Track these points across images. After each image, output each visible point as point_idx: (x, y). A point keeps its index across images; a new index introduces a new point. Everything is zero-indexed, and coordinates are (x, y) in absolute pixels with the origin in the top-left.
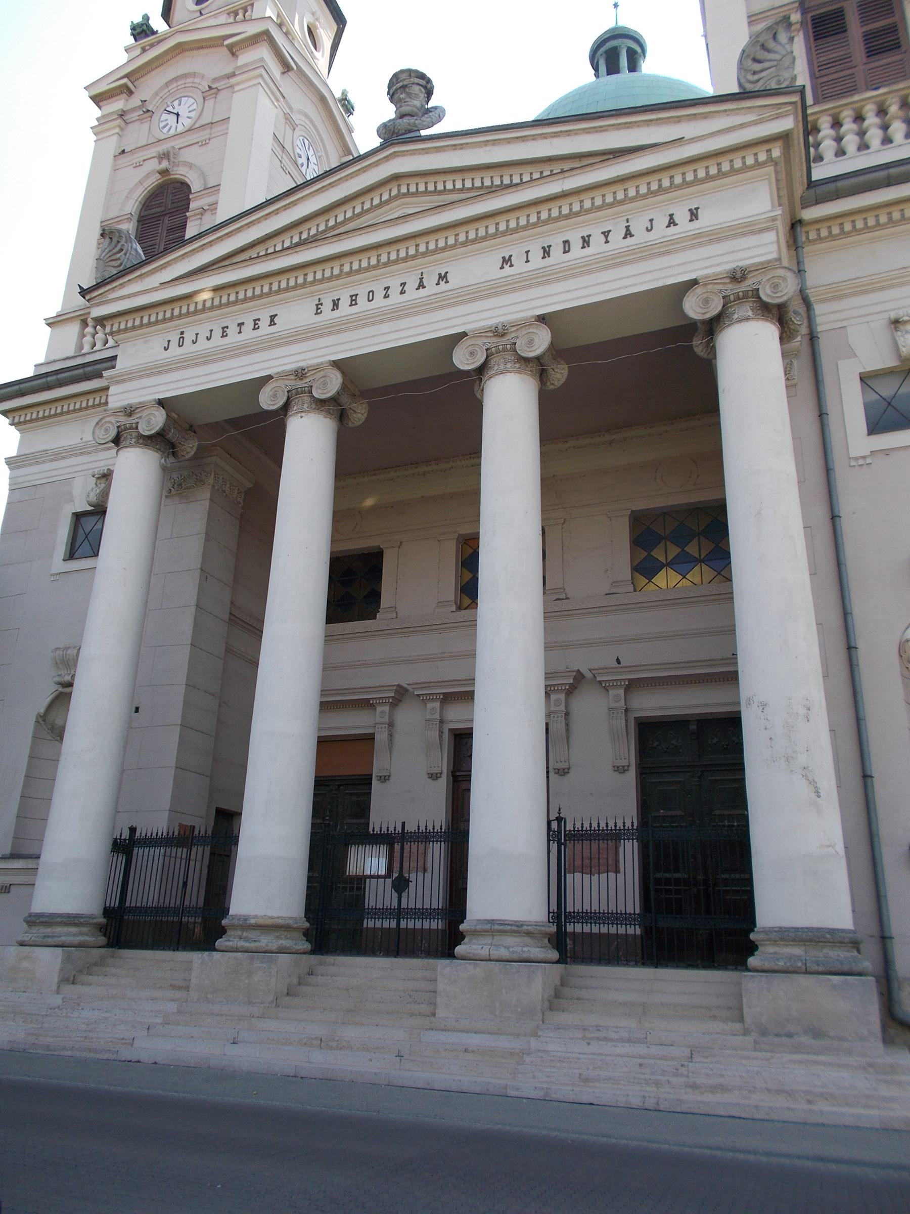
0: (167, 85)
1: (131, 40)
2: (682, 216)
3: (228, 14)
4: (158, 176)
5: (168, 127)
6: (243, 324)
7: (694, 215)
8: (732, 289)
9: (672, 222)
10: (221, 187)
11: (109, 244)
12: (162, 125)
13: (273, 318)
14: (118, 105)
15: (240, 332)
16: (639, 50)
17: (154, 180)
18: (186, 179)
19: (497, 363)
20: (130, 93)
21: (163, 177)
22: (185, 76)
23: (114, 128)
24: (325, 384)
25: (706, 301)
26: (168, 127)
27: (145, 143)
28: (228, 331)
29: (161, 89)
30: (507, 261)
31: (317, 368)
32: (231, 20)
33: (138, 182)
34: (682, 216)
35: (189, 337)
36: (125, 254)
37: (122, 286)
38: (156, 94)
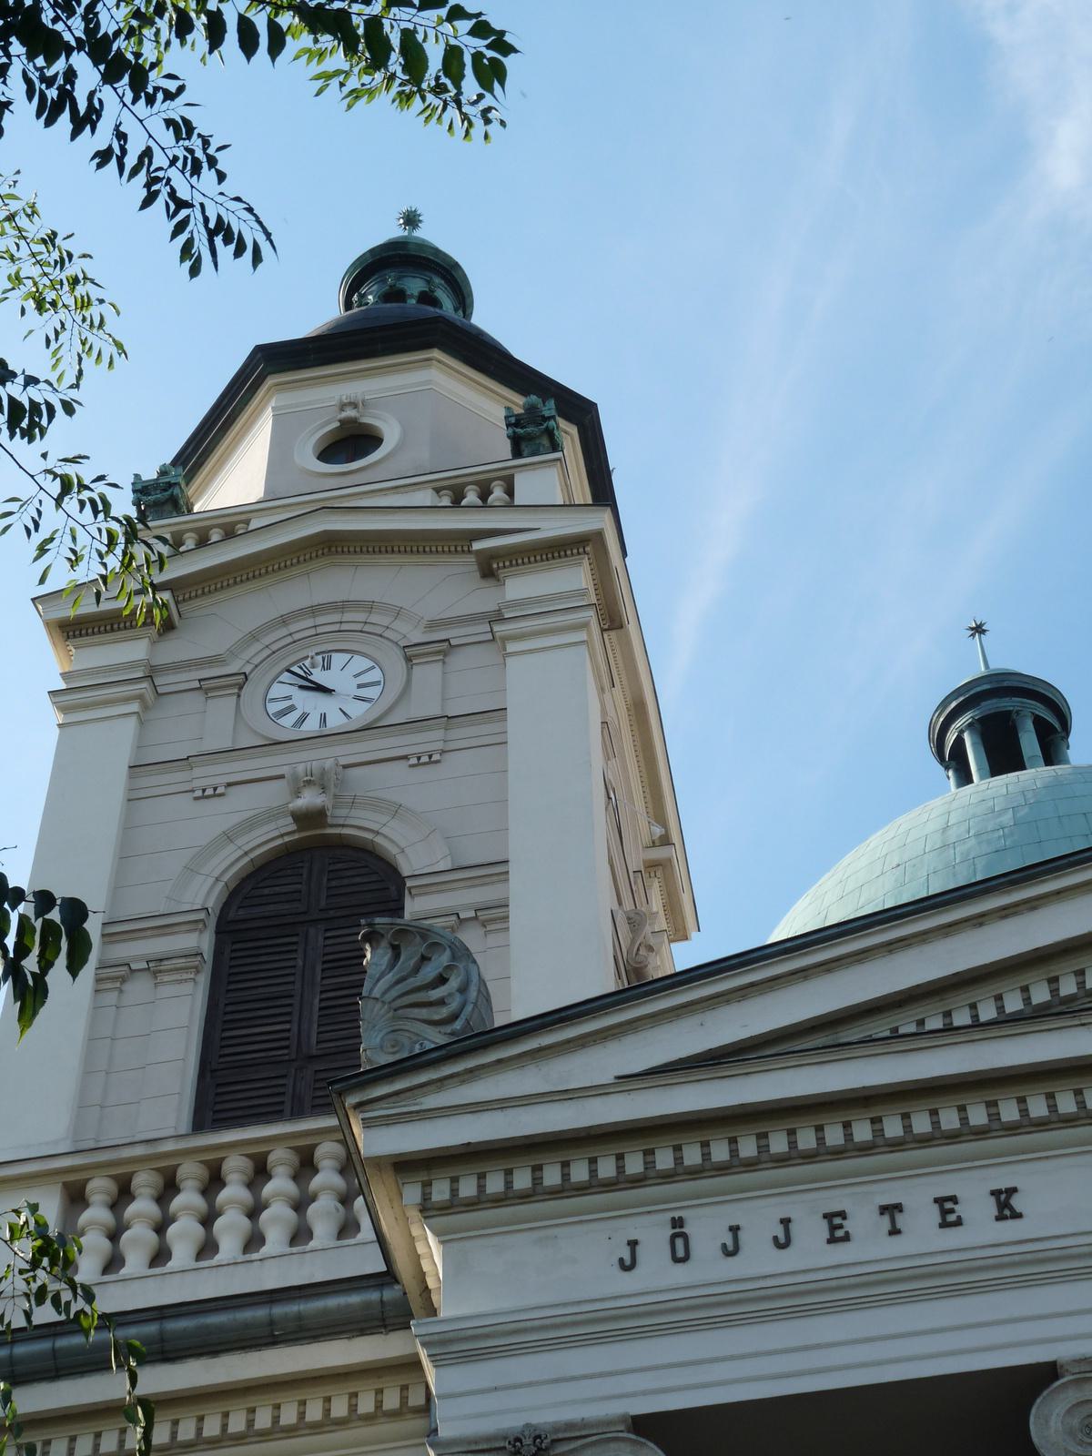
0: (284, 620)
3: (438, 490)
4: (288, 824)
5: (293, 717)
6: (898, 1208)
10: (512, 868)
11: (392, 965)
12: (273, 708)
15: (895, 1231)
18: (379, 840)
20: (168, 626)
21: (299, 830)
22: (342, 606)
23: (127, 700)
26: (293, 717)
27: (228, 745)
28: (849, 1225)
32: (446, 501)
35: (706, 1229)
36: (463, 990)
37: (472, 1074)
38: (253, 637)
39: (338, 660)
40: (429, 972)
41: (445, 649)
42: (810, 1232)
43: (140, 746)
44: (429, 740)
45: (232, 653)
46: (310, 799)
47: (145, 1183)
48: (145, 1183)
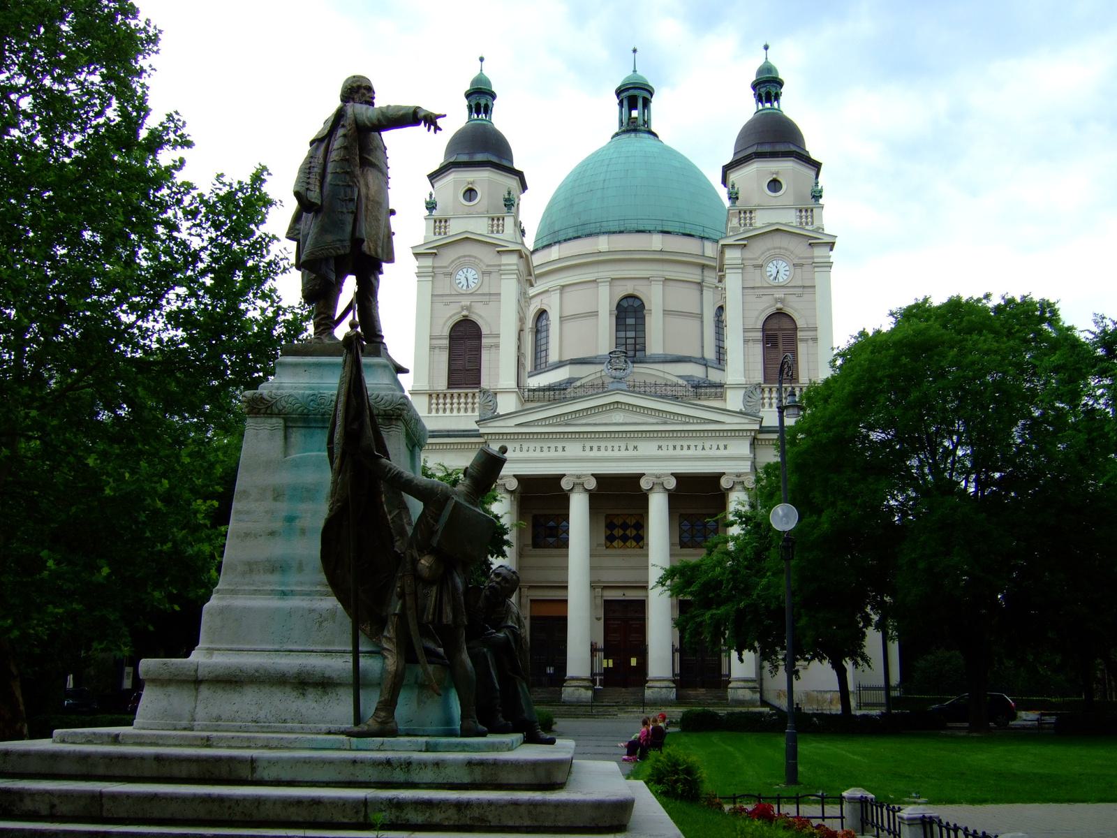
0: (459, 258)
1: (427, 213)
2: (722, 447)
7: (725, 447)
8: (737, 479)
9: (718, 448)
12: (458, 281)
13: (564, 448)
14: (428, 262)
16: (648, 96)
17: (457, 318)
19: (657, 488)
22: (469, 256)
23: (429, 276)
24: (589, 483)
25: (728, 482)
29: (455, 260)
30: (660, 447)
31: (585, 475)
33: (449, 316)
34: (722, 447)
35: (525, 447)
38: (453, 262)
39: (470, 270)
40: (489, 399)
41: (490, 273)
42: (538, 449)
43: (432, 291)
44: (486, 298)
45: (449, 265)
46: (465, 313)
47: (441, 396)
48: (441, 396)
